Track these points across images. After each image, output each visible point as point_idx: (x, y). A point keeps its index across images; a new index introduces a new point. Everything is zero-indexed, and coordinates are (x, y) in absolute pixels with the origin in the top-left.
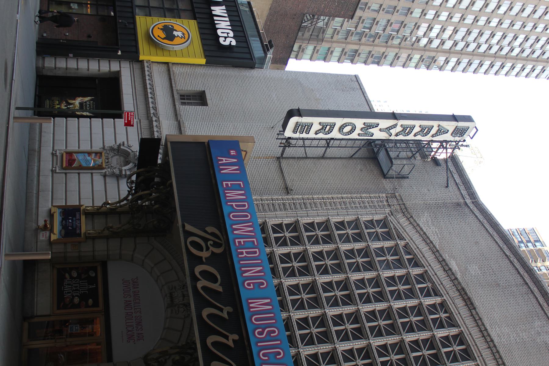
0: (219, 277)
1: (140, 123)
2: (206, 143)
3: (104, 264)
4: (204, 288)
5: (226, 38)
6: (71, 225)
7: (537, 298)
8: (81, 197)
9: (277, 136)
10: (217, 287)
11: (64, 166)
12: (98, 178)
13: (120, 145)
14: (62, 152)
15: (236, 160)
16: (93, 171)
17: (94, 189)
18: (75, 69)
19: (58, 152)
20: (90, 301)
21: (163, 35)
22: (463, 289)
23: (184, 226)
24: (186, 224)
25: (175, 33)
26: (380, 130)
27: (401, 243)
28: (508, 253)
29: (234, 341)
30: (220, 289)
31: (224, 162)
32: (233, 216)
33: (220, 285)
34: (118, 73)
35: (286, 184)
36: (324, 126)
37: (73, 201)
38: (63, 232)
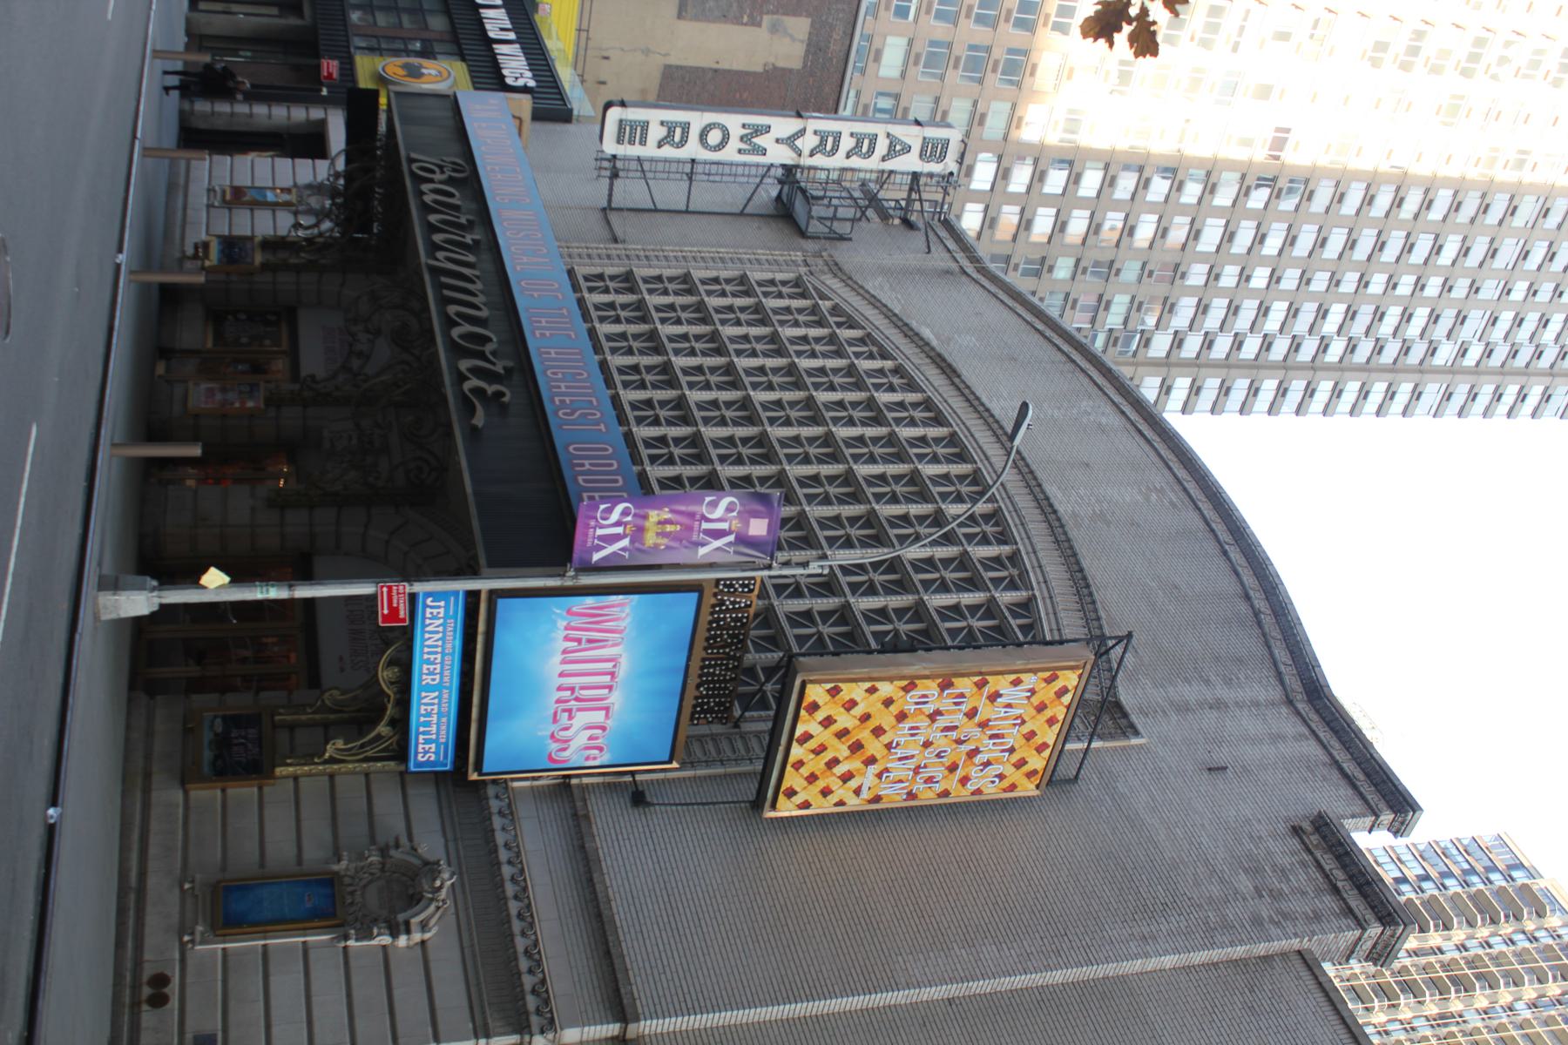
3: (289, 315)
7: (1091, 378)
9: (595, 173)
21: (401, 72)
22: (939, 355)
26: (777, 141)
27: (825, 305)
28: (1040, 326)
34: (323, 123)
36: (671, 127)
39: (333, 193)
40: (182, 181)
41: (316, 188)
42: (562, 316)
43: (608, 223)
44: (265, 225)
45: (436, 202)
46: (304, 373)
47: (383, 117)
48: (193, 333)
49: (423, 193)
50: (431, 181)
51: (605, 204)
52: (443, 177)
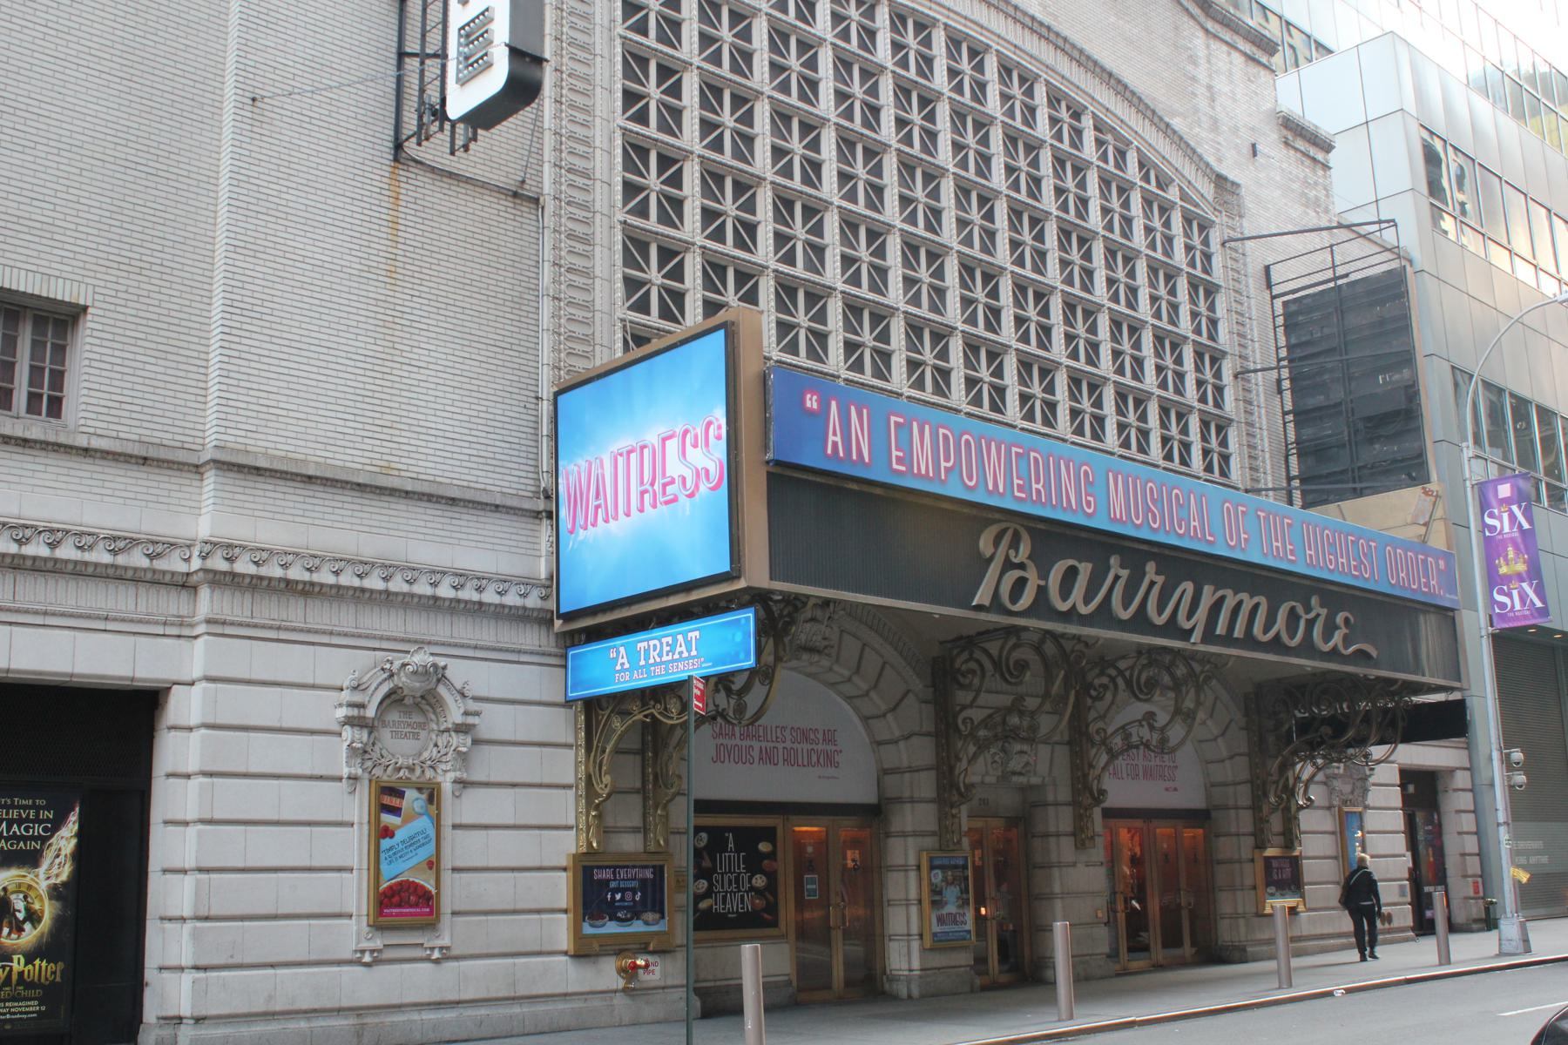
0: (1071, 562)
1: (224, 623)
4: (1087, 600)
6: (629, 895)
8: (537, 863)
12: (473, 806)
15: (834, 404)
16: (448, 820)
17: (511, 822)
19: (365, 945)
20: (764, 847)
23: (980, 608)
31: (838, 439)
32: (971, 479)
35: (499, 190)
37: (560, 889)
38: (650, 916)
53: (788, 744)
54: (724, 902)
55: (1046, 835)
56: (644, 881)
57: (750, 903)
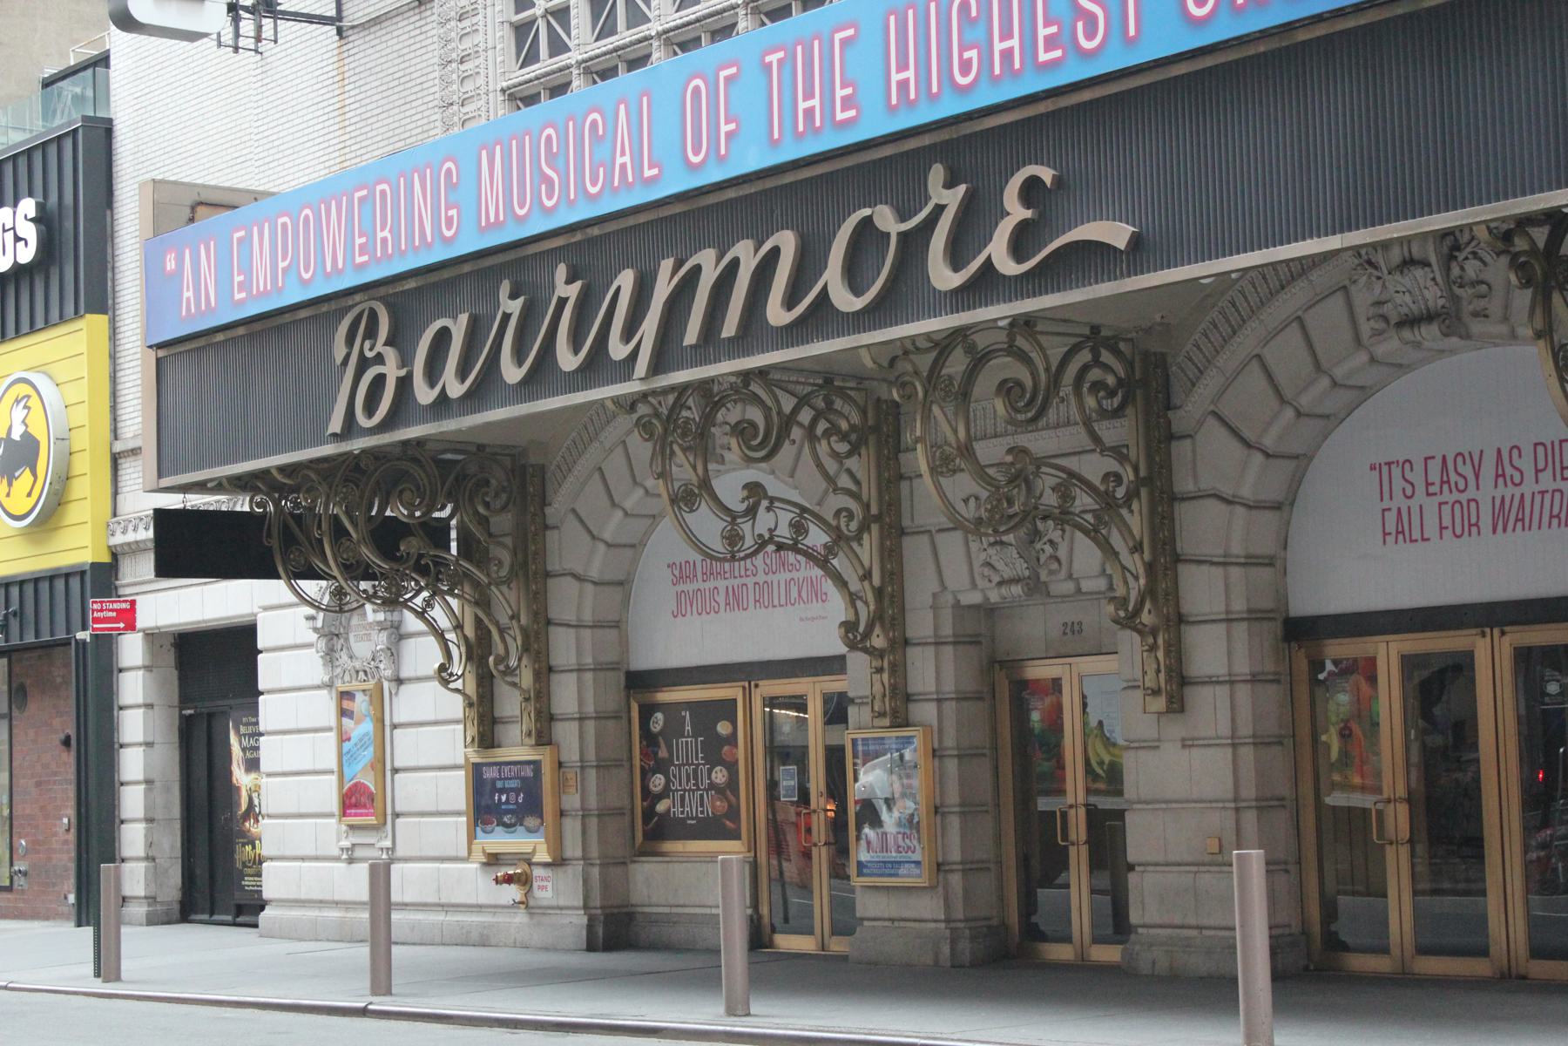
2: (161, 353)
3: (641, 682)
5: (17, 239)
10: (459, 331)
11: (372, 820)
13: (315, 630)
14: (344, 828)
17: (432, 718)
18: (147, 792)
20: (723, 728)
21: (26, 477)
24: (330, 431)
25: (16, 436)
29: (569, 282)
30: (464, 318)
33: (455, 318)
34: (153, 637)
38: (531, 821)
39: (340, 604)
40: (334, 914)
41: (333, 641)
42: (788, 62)
43: (376, 21)
44: (432, 733)
45: (462, 374)
46: (833, 645)
47: (197, 501)
48: (707, 880)
49: (443, 396)
50: (405, 384)
51: (331, 30)
52: (391, 355)
53: (761, 578)
54: (683, 806)
55: (1254, 679)
56: (524, 779)
57: (714, 806)
